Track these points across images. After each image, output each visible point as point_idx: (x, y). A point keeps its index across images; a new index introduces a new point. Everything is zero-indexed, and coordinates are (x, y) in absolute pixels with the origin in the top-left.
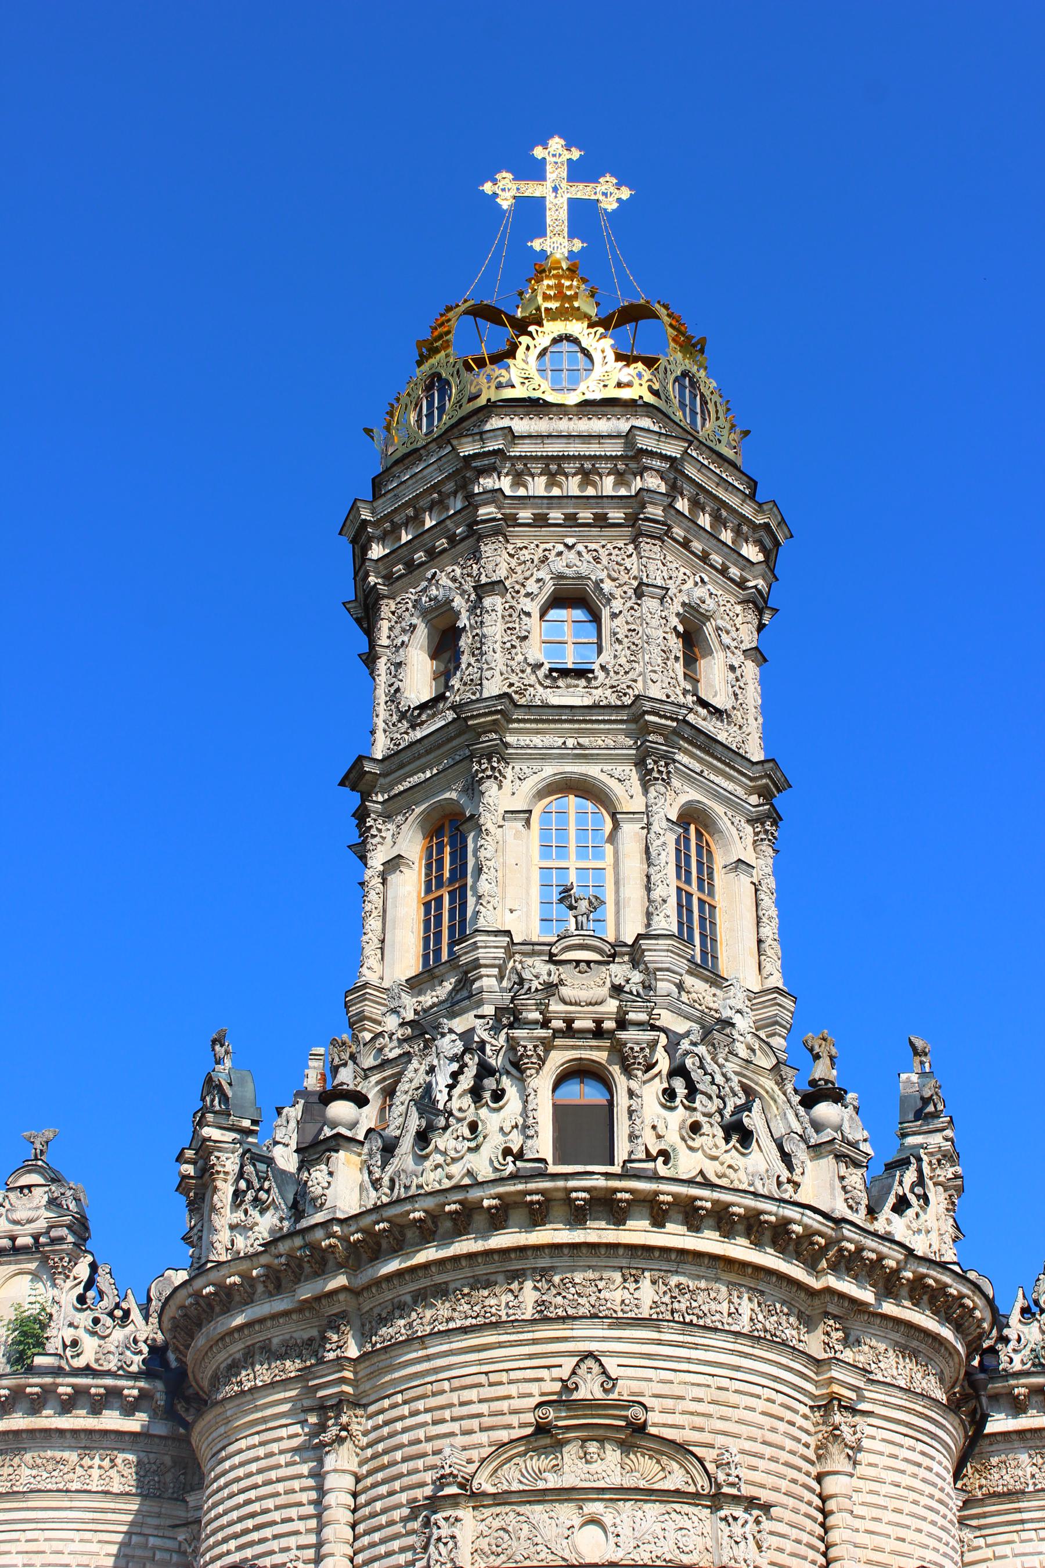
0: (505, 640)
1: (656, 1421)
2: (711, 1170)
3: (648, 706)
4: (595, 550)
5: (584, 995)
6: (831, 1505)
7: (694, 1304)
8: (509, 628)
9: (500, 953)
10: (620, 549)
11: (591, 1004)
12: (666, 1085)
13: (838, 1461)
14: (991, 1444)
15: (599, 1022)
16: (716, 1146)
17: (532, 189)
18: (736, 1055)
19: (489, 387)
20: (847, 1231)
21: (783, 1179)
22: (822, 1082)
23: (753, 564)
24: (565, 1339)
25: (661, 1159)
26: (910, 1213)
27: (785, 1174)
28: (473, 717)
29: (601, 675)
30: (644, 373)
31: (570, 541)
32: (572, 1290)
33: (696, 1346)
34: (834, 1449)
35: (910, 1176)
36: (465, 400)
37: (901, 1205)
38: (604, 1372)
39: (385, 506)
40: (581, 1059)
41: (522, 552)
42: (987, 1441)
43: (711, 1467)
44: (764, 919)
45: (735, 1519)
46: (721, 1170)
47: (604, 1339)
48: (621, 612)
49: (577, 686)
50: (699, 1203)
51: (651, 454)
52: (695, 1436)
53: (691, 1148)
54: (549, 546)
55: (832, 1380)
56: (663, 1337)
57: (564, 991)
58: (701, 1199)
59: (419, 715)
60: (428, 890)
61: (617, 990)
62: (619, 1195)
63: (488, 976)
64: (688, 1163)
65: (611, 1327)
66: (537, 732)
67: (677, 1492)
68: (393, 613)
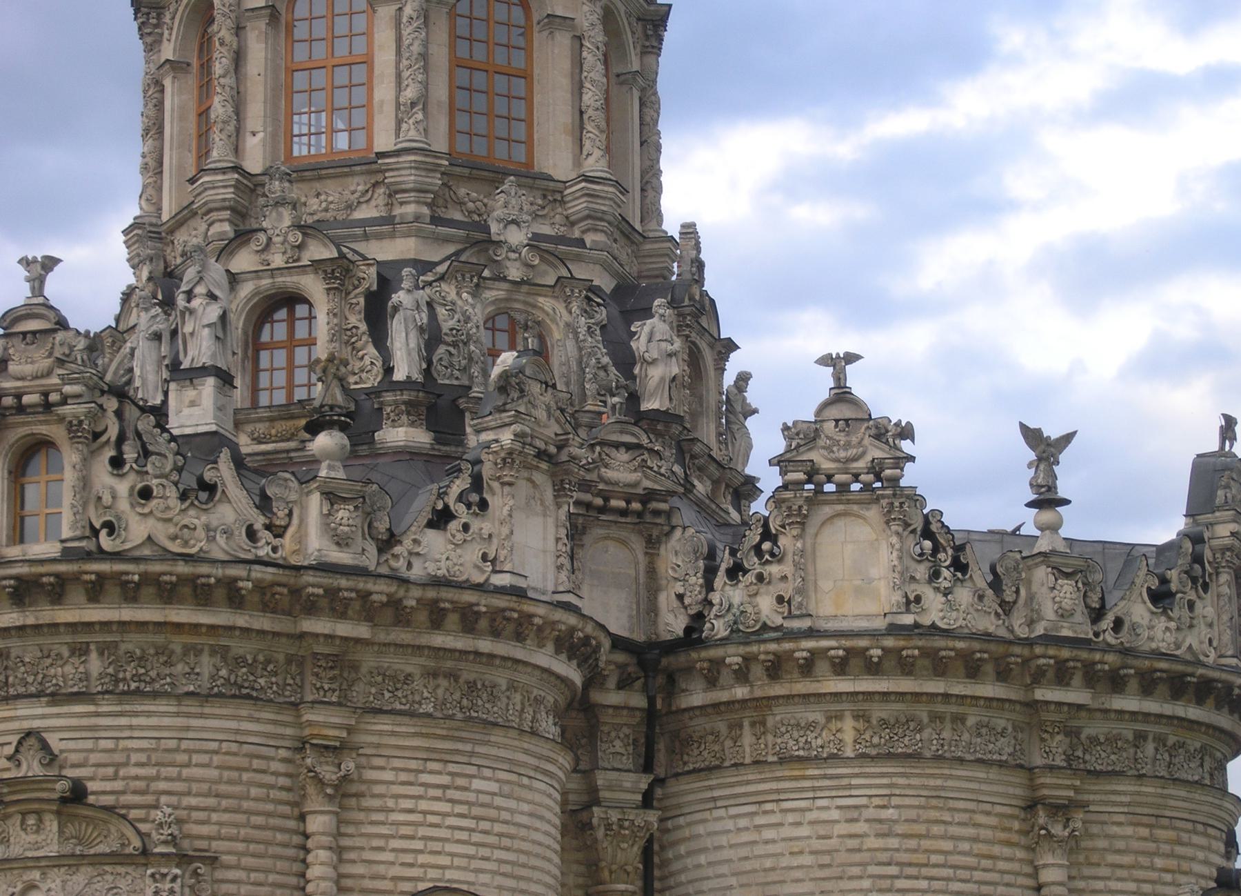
1: (94, 789)
2: (162, 533)
5: (28, 369)
6: (310, 844)
7: (142, 671)
9: (229, 194)
11: (37, 377)
12: (113, 453)
13: (315, 802)
14: (691, 719)
15: (46, 394)
16: (168, 508)
18: (504, 279)
20: (309, 578)
21: (258, 526)
22: (327, 408)
24: (11, 719)
25: (104, 532)
26: (454, 526)
27: (259, 521)
32: (22, 669)
33: (136, 714)
34: (311, 790)
35: (460, 484)
37: (441, 519)
38: (45, 746)
40: (33, 434)
42: (686, 715)
43: (144, 827)
44: (587, 85)
45: (164, 876)
46: (172, 530)
47: (43, 717)
50: (124, 578)
52: (137, 799)
53: (141, 514)
55: (310, 724)
56: (100, 709)
57: (12, 368)
58: (127, 573)
61: (61, 362)
62: (45, 580)
63: (221, 221)
64: (137, 530)
65: (49, 704)
67: (112, 854)
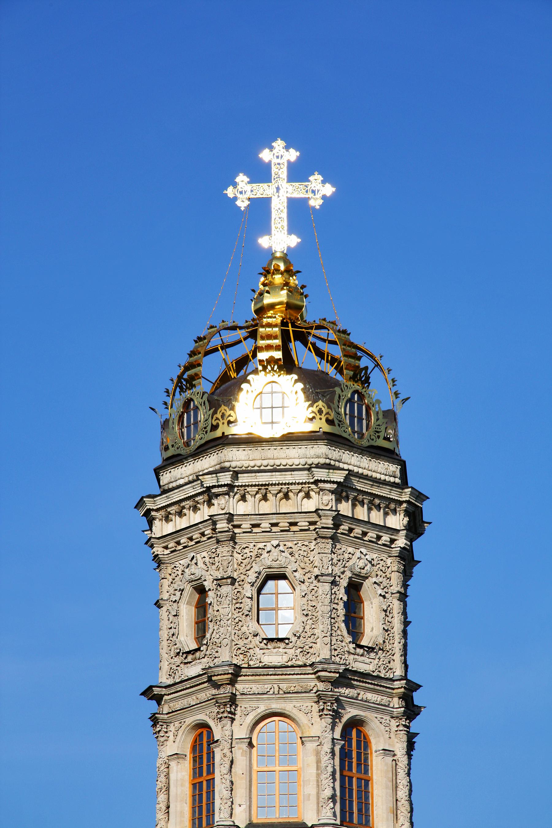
0: (235, 617)
3: (320, 667)
4: (291, 548)
8: (237, 608)
10: (307, 546)
17: (262, 190)
19: (223, 423)
23: (398, 531)
28: (215, 675)
29: (294, 639)
30: (323, 409)
31: (275, 543)
36: (209, 428)
39: (162, 501)
41: (245, 551)
48: (306, 594)
49: (279, 648)
51: (325, 482)
54: (261, 545)
59: (186, 658)
60: (194, 777)
66: (254, 681)
68: (170, 575)
